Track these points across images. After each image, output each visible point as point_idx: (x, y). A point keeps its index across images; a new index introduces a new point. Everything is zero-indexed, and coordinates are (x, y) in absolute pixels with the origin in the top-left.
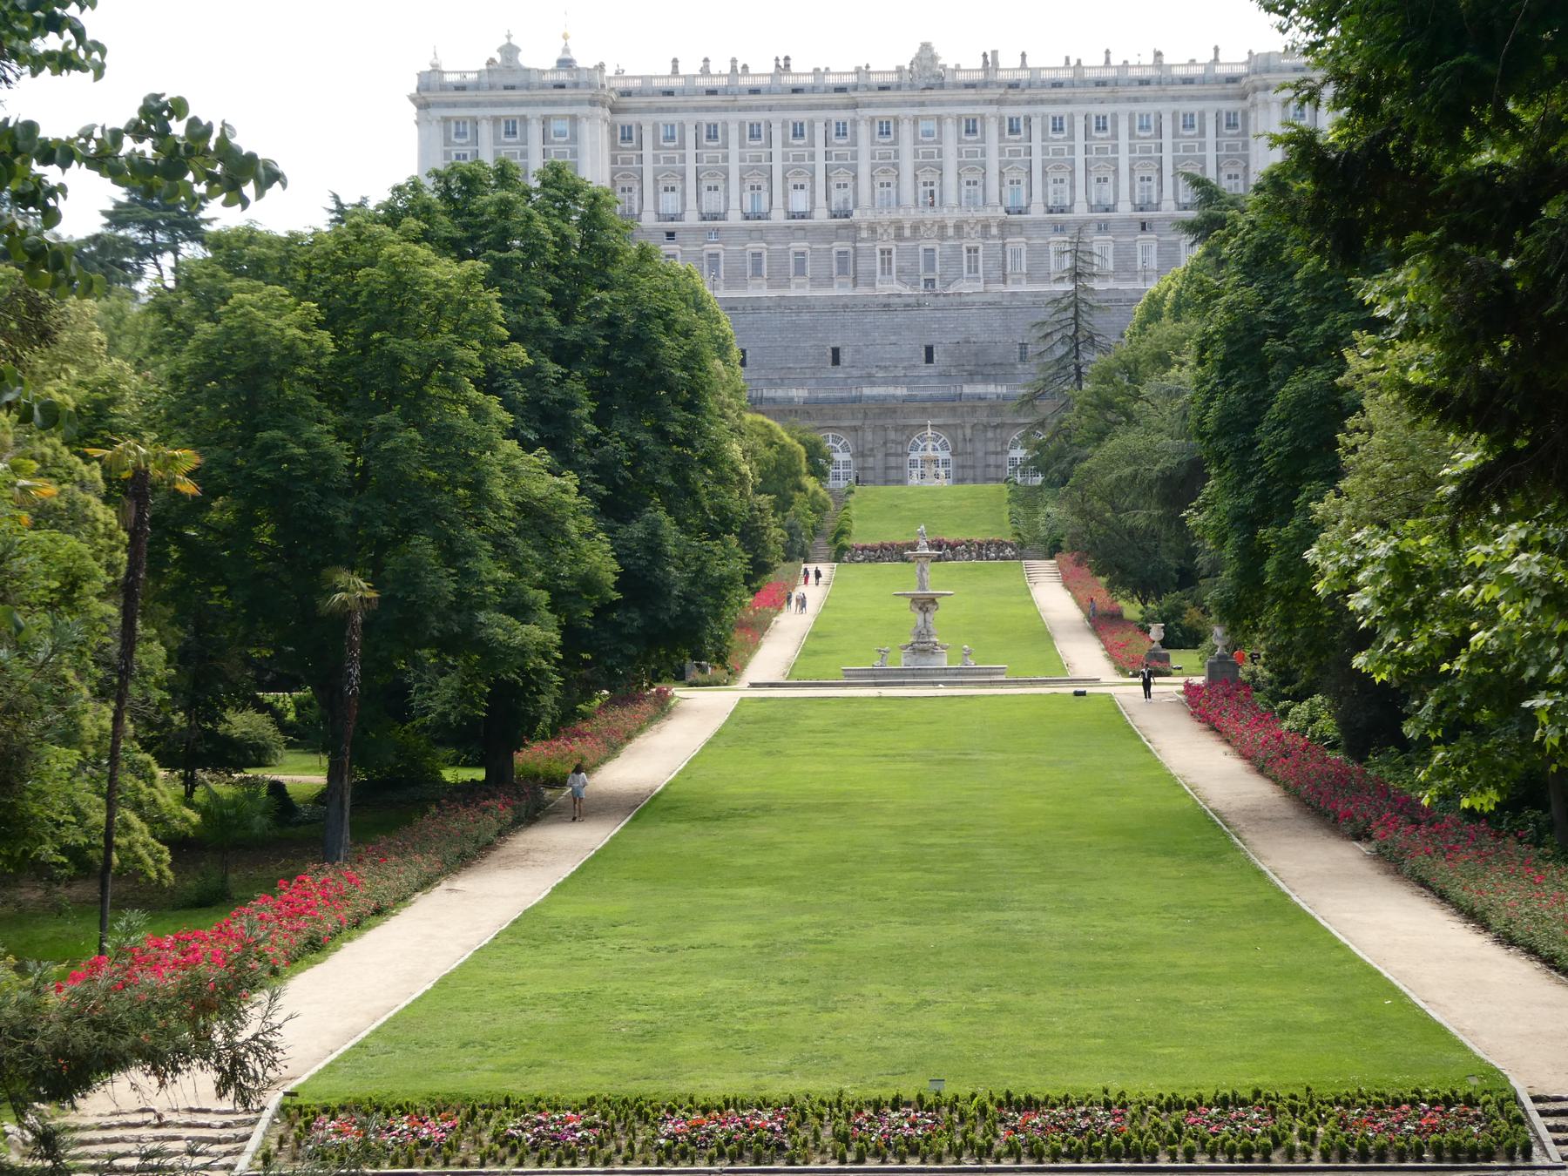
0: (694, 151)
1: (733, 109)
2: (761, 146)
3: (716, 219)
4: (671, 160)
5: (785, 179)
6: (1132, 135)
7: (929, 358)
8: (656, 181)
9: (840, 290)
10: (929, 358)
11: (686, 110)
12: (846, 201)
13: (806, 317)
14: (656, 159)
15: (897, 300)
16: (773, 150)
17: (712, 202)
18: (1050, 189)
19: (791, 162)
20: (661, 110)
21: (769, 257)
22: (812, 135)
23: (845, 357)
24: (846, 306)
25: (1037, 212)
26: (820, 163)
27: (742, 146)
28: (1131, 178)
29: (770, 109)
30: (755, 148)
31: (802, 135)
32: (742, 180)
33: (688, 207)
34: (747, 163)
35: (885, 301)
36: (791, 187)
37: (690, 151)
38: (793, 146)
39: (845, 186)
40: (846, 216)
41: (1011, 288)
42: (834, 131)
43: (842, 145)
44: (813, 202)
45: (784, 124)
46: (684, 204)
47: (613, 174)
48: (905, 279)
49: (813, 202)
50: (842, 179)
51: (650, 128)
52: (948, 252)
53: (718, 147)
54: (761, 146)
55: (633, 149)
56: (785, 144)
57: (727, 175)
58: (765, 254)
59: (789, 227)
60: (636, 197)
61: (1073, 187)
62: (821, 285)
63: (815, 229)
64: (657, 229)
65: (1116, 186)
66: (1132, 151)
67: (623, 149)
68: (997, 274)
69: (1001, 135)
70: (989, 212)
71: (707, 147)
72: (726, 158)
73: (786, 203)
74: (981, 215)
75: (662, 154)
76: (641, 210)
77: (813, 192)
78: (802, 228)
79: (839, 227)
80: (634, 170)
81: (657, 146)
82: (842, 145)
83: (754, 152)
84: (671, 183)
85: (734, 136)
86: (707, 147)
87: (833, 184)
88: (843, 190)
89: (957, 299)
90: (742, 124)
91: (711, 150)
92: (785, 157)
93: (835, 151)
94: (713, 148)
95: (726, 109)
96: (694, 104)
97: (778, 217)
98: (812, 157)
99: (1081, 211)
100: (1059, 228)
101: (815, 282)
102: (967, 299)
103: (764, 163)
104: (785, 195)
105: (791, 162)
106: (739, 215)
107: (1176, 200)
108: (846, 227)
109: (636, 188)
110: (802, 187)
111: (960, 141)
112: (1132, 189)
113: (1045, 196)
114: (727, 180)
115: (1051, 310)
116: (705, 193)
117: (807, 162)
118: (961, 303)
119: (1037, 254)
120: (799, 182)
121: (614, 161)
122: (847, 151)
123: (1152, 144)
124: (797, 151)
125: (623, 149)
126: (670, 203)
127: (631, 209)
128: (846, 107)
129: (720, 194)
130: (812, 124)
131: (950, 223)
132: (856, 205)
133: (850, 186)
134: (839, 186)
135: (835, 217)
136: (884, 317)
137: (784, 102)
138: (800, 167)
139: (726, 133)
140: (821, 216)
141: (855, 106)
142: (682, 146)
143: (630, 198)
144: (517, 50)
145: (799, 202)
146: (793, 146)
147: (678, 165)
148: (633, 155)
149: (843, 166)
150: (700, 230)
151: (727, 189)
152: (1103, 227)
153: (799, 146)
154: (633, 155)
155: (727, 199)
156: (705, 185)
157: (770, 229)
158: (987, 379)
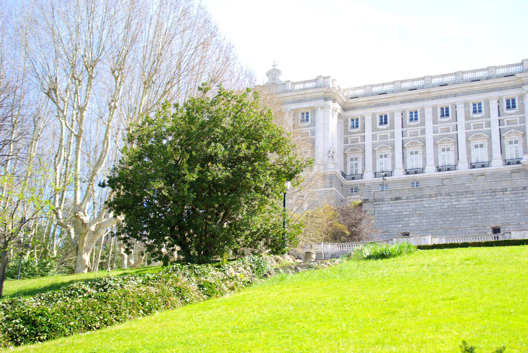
0: (400, 130)
1: (428, 99)
2: (449, 121)
3: (416, 173)
4: (385, 137)
5: (468, 141)
8: (374, 152)
11: (394, 103)
12: (517, 151)
14: (374, 137)
16: (458, 123)
17: (414, 162)
19: (472, 129)
20: (378, 105)
22: (488, 109)
24: (504, 190)
27: (435, 122)
29: (455, 96)
30: (446, 122)
31: (480, 111)
32: (435, 145)
33: (396, 167)
34: (440, 134)
36: (472, 146)
37: (398, 130)
38: (473, 119)
39: (516, 142)
40: (518, 163)
42: (505, 105)
43: (512, 114)
44: (490, 155)
45: (466, 105)
46: (393, 166)
47: (345, 150)
50: (513, 138)
51: (370, 118)
53: (418, 125)
54: (449, 121)
55: (359, 132)
56: (467, 118)
57: (424, 143)
59: (472, 174)
60: (360, 163)
63: (493, 174)
64: (374, 183)
67: (351, 133)
71: (410, 126)
72: (423, 132)
73: (469, 158)
76: (364, 170)
77: (490, 149)
78: (483, 175)
79: (512, 172)
80: (359, 146)
81: (374, 129)
82: (512, 114)
83: (444, 126)
84: (384, 152)
85: (429, 116)
86: (410, 126)
87: (506, 142)
88: (514, 145)
90: (434, 109)
91: (413, 127)
92: (467, 127)
93: (506, 119)
94: (414, 126)
95: (423, 100)
96: (400, 99)
97: (463, 168)
98: (489, 124)
103: (451, 133)
104: (469, 152)
105: (472, 129)
106: (434, 168)
108: (518, 171)
109: (360, 157)
110: (481, 146)
114: (424, 146)
116: (409, 157)
117: (485, 129)
120: (478, 143)
121: (346, 141)
122: (517, 117)
124: (476, 122)
125: (351, 133)
126: (384, 165)
127: (356, 171)
128: (514, 87)
129: (420, 157)
130: (487, 102)
133: (521, 141)
134: (511, 143)
135: (509, 164)
137: (465, 90)
138: (479, 132)
139: (423, 115)
140: (497, 164)
141: (520, 86)
143: (356, 165)
144: (279, 72)
146: (473, 119)
147: (389, 140)
148: (358, 136)
149: (514, 128)
150: (406, 181)
151: (424, 153)
153: (478, 118)
154: (358, 136)
155: (425, 159)
156: (408, 151)
157: (456, 177)
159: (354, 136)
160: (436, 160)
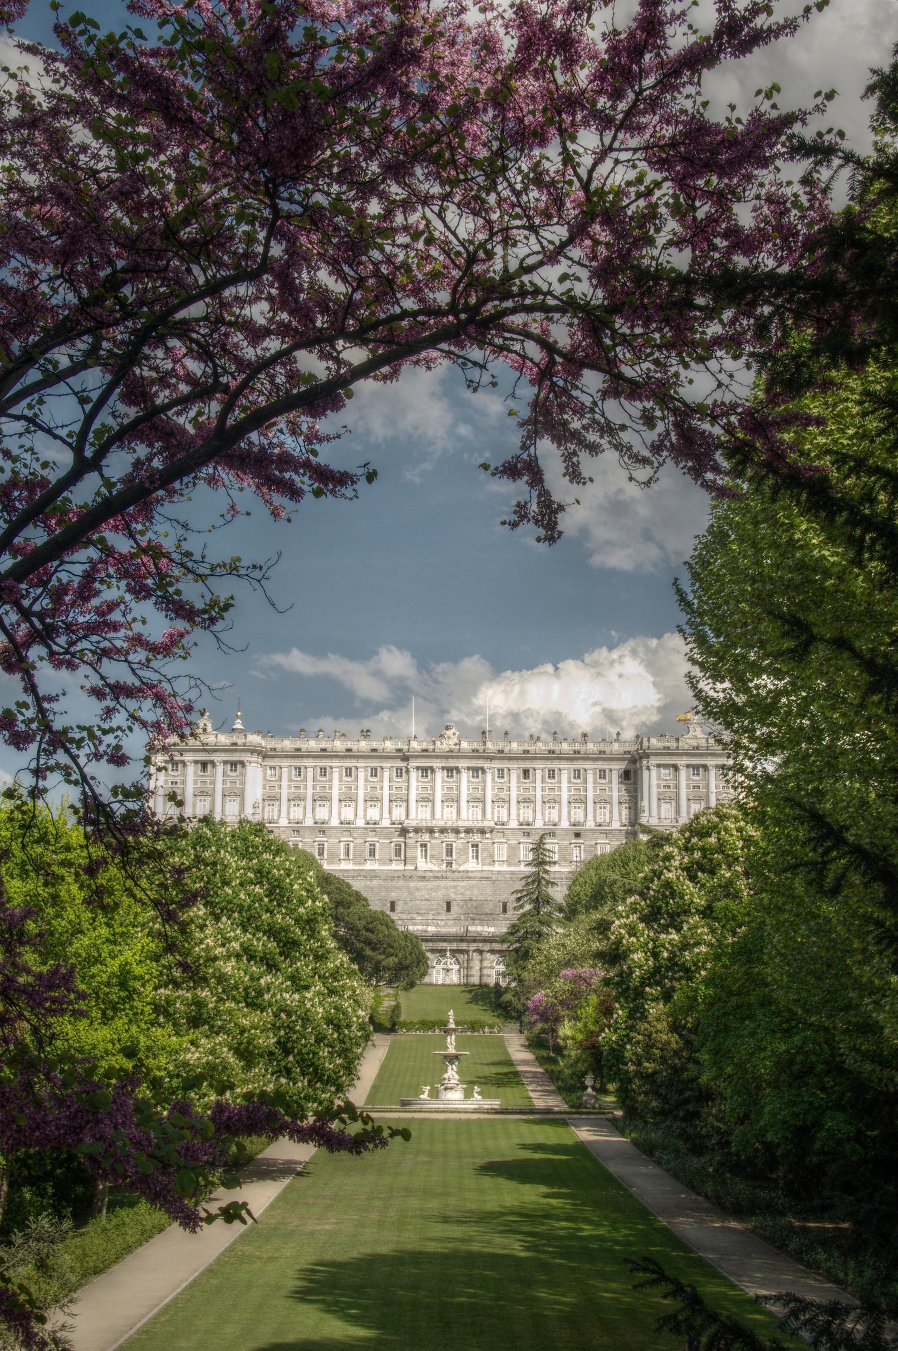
6: (569, 782)
7: (448, 909)
9: (397, 866)
10: (448, 909)
13: (375, 882)
15: (430, 874)
17: (322, 813)
18: (521, 812)
21: (355, 847)
23: (399, 908)
25: (514, 824)
26: (386, 792)
27: (340, 780)
28: (569, 808)
35: (423, 874)
41: (497, 867)
44: (381, 815)
48: (434, 861)
49: (381, 815)
52: (461, 846)
58: (352, 845)
59: (366, 829)
60: (276, 809)
61: (534, 811)
62: (384, 864)
65: (560, 811)
66: (570, 791)
68: (488, 860)
69: (493, 779)
70: (486, 824)
72: (331, 788)
73: (365, 815)
74: (480, 825)
75: (293, 784)
76: (279, 816)
77: (381, 809)
89: (465, 875)
93: (395, 785)
98: (382, 788)
99: (539, 824)
100: (527, 834)
101: (382, 861)
102: (470, 875)
104: (365, 810)
107: (595, 820)
111: (469, 781)
112: (569, 813)
113: (518, 815)
115: (523, 883)
118: (467, 876)
119: (513, 850)
121: (264, 788)
123: (581, 787)
131: (462, 830)
132: (407, 816)
136: (421, 884)
140: (386, 823)
142: (305, 780)
145: (373, 813)
151: (331, 807)
152: (553, 834)
155: (330, 812)
158: (482, 922)
159: (272, 784)
160: (340, 814)
